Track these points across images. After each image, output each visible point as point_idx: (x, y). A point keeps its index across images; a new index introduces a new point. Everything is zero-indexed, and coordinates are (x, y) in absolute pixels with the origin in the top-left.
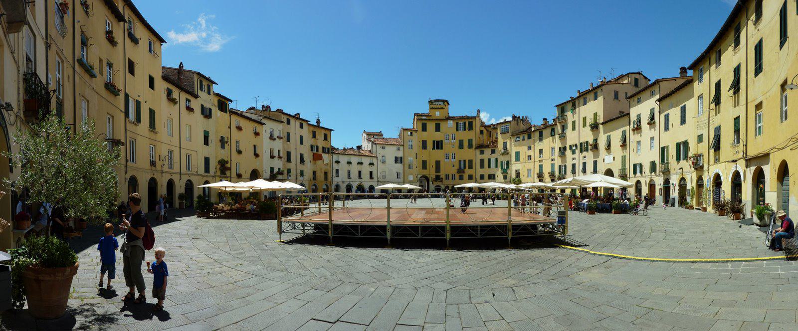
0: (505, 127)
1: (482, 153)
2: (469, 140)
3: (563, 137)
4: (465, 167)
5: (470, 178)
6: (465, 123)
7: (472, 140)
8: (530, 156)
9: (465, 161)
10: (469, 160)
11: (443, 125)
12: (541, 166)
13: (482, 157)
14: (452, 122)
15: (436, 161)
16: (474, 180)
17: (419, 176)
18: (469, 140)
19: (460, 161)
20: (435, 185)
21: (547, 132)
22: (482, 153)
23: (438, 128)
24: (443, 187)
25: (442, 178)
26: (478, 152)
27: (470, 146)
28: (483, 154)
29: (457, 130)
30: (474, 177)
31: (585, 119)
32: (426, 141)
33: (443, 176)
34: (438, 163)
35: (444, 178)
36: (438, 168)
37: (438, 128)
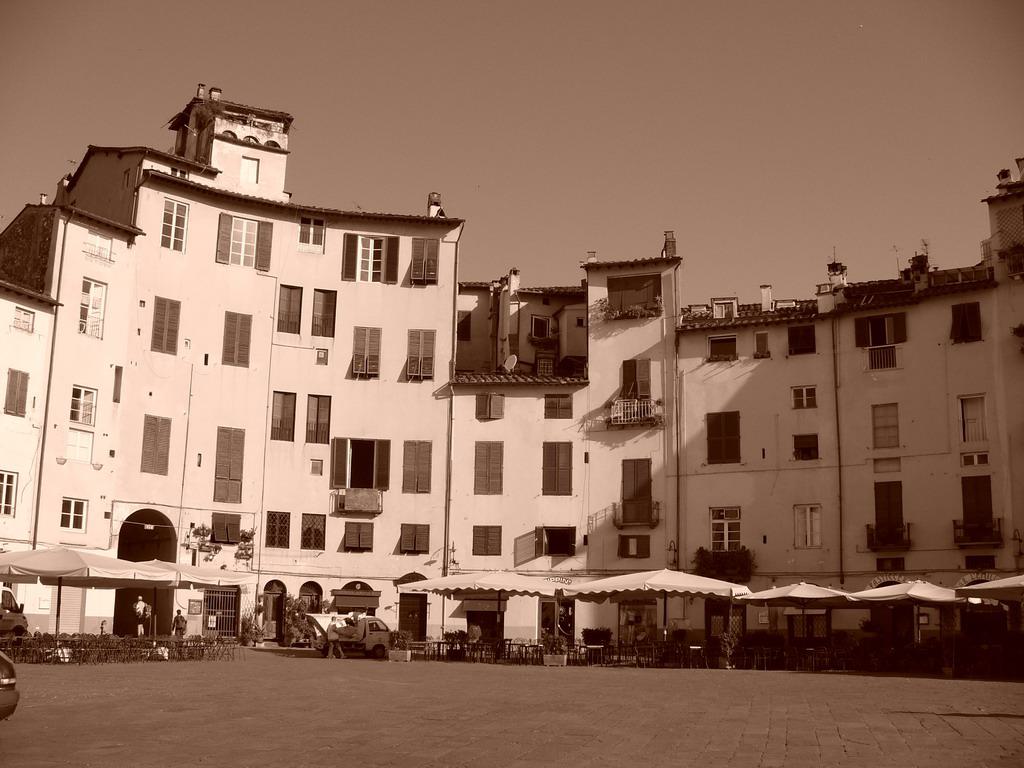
2: (414, 336)
6: (393, 244)
7: (430, 336)
10: (408, 445)
12: (888, 496)
13: (489, 431)
15: (224, 433)
17: (123, 513)
18: (414, 336)
25: (247, 537)
26: (465, 404)
27: (417, 370)
29: (349, 272)
32: (175, 306)
33: (253, 521)
34: (230, 443)
35: (259, 539)
36: (228, 481)
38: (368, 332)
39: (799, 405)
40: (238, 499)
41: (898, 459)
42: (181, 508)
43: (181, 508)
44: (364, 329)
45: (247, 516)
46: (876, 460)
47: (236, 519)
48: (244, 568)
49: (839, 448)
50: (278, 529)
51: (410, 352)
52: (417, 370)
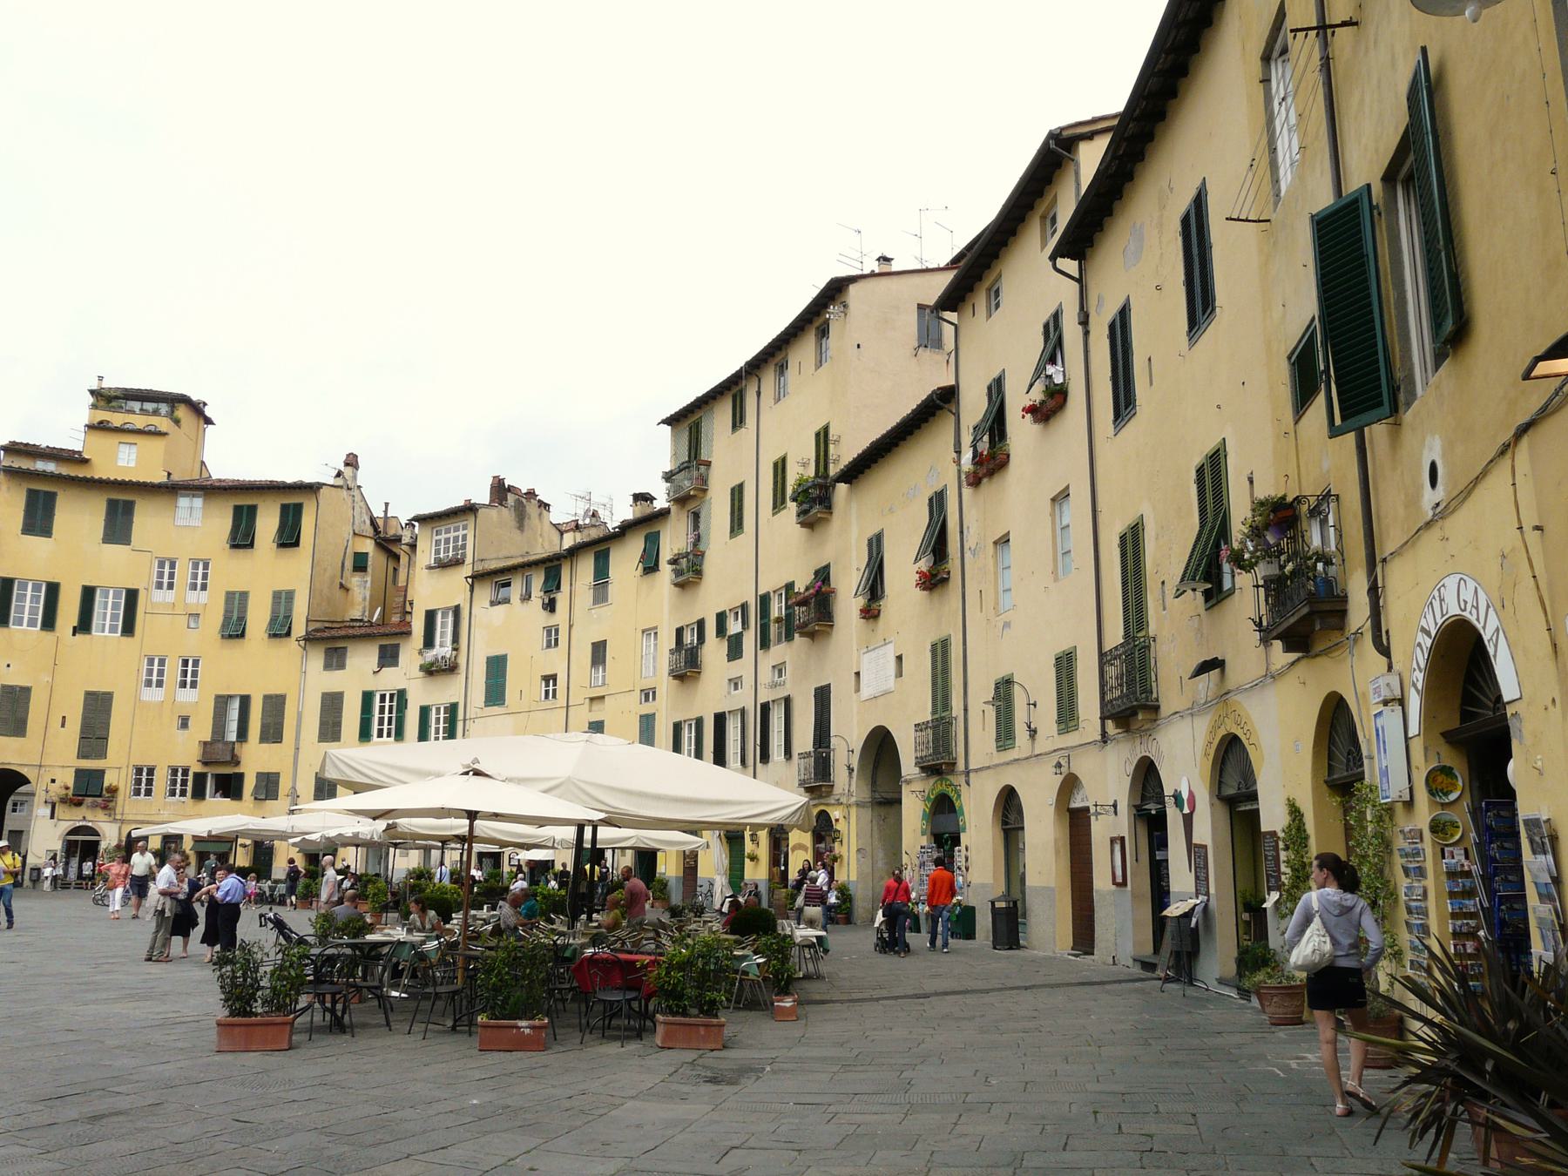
0: (452, 535)
1: (335, 659)
2: (277, 595)
3: (690, 571)
4: (243, 733)
5: (268, 786)
7: (290, 595)
8: (550, 679)
9: (245, 701)
10: (266, 698)
11: (147, 520)
13: (334, 681)
14: (198, 502)
16: (282, 802)
18: (277, 595)
19: (222, 702)
20: (67, 826)
21: (626, 559)
22: (335, 659)
23: (118, 527)
24: (110, 835)
25: (113, 791)
26: (317, 659)
27: (280, 629)
28: (341, 666)
30: (284, 786)
31: (780, 467)
34: (98, 707)
37: (118, 527)
38: (237, 596)
39: (549, 646)
40: (102, 753)
41: (603, 697)
42: (40, 766)
43: (40, 766)
44: (233, 593)
45: (112, 771)
46: (592, 699)
47: (101, 773)
48: (106, 818)
49: (568, 688)
50: (144, 778)
51: (273, 612)
52: (280, 629)
